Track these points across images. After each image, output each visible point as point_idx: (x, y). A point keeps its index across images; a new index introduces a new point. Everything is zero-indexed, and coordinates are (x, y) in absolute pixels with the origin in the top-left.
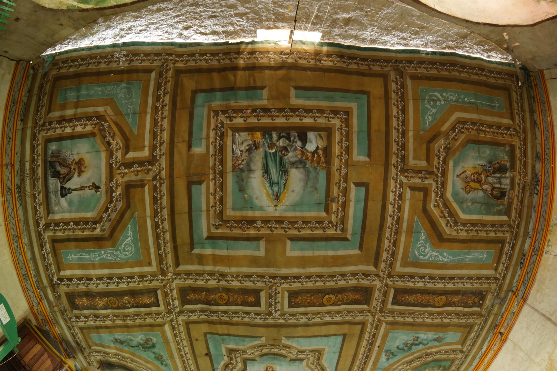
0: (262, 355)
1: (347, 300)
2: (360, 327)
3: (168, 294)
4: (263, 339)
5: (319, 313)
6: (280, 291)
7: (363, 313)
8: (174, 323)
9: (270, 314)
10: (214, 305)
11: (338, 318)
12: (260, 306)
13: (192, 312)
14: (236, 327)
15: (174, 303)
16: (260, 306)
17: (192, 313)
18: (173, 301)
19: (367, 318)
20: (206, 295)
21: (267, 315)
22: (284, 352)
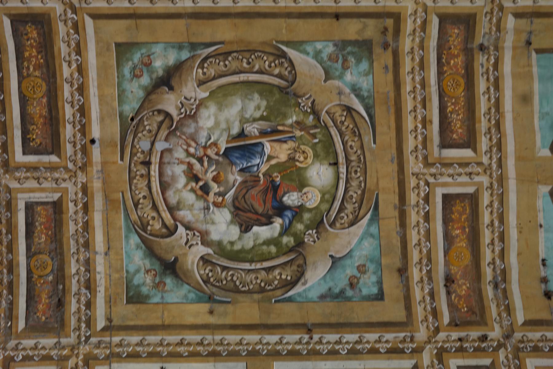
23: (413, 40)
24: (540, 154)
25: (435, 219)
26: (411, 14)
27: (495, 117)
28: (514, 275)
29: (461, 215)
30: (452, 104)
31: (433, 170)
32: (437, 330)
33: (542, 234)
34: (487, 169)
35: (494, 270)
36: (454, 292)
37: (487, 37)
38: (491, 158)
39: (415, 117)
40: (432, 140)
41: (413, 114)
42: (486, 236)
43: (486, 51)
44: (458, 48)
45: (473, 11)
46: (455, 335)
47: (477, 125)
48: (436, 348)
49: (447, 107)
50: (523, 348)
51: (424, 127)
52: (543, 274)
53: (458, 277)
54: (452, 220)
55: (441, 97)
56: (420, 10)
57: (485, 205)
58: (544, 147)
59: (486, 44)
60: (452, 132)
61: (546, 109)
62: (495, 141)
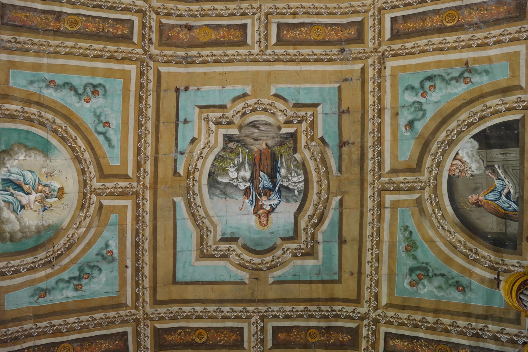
0: (273, 249)
1: (180, 334)
2: (160, 297)
3: (371, 345)
4: (271, 280)
5: (210, 317)
6: (252, 349)
7: (159, 317)
8: (374, 303)
9: (262, 318)
10: (322, 327)
11: (187, 309)
12: (273, 328)
13: (349, 318)
14: (302, 297)
15: (367, 333)
16: (273, 328)
17: (349, 315)
18: (368, 335)
19: (153, 310)
20: (329, 341)
21: (266, 317)
22: (247, 257)
23: (347, 7)
24: (272, 87)
25: (230, 20)
26: (363, 3)
27: (298, 59)
28: (191, 69)
29: (233, 35)
30: (306, 31)
31: (263, 18)
32: (157, 13)
33: (218, 88)
34: (262, 52)
35: (195, 56)
36: (181, 30)
37: (350, 52)
38: (270, 55)
39: (298, 8)
40: (283, 18)
41: (300, 6)
42: (218, 52)
43: (340, 53)
44: (342, 36)
45: (365, 42)
46: (153, 24)
47: (292, 47)
48: (146, 10)
49: (304, 27)
50: (143, 65)
51: (291, 14)
52: (191, 88)
53: (192, 33)
54: (229, 30)
55: (311, 24)
56: (366, 8)
57: (239, 51)
58: (276, 89)
59: (344, 53)
60: (288, 31)
61: (302, 92)
62: (281, 57)
